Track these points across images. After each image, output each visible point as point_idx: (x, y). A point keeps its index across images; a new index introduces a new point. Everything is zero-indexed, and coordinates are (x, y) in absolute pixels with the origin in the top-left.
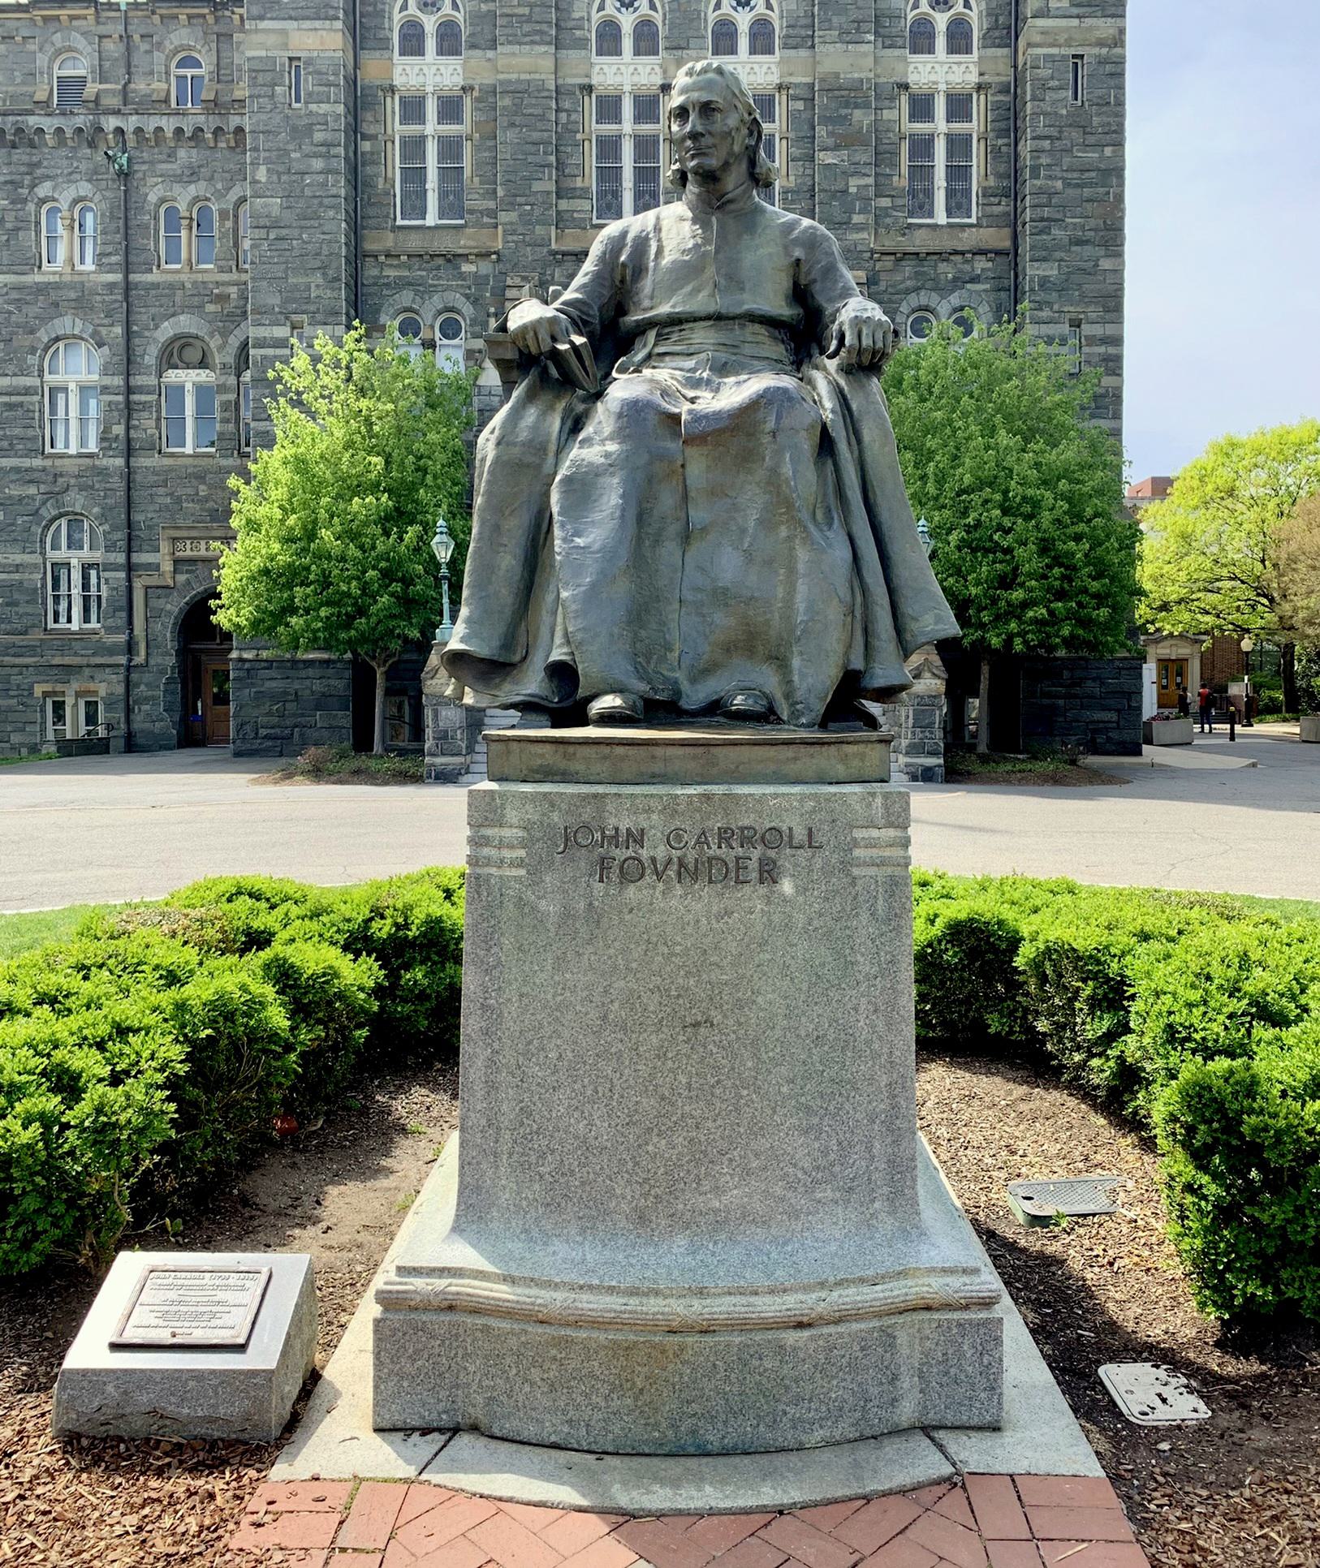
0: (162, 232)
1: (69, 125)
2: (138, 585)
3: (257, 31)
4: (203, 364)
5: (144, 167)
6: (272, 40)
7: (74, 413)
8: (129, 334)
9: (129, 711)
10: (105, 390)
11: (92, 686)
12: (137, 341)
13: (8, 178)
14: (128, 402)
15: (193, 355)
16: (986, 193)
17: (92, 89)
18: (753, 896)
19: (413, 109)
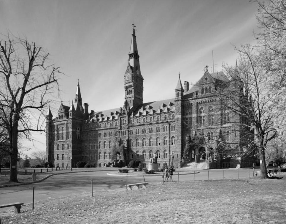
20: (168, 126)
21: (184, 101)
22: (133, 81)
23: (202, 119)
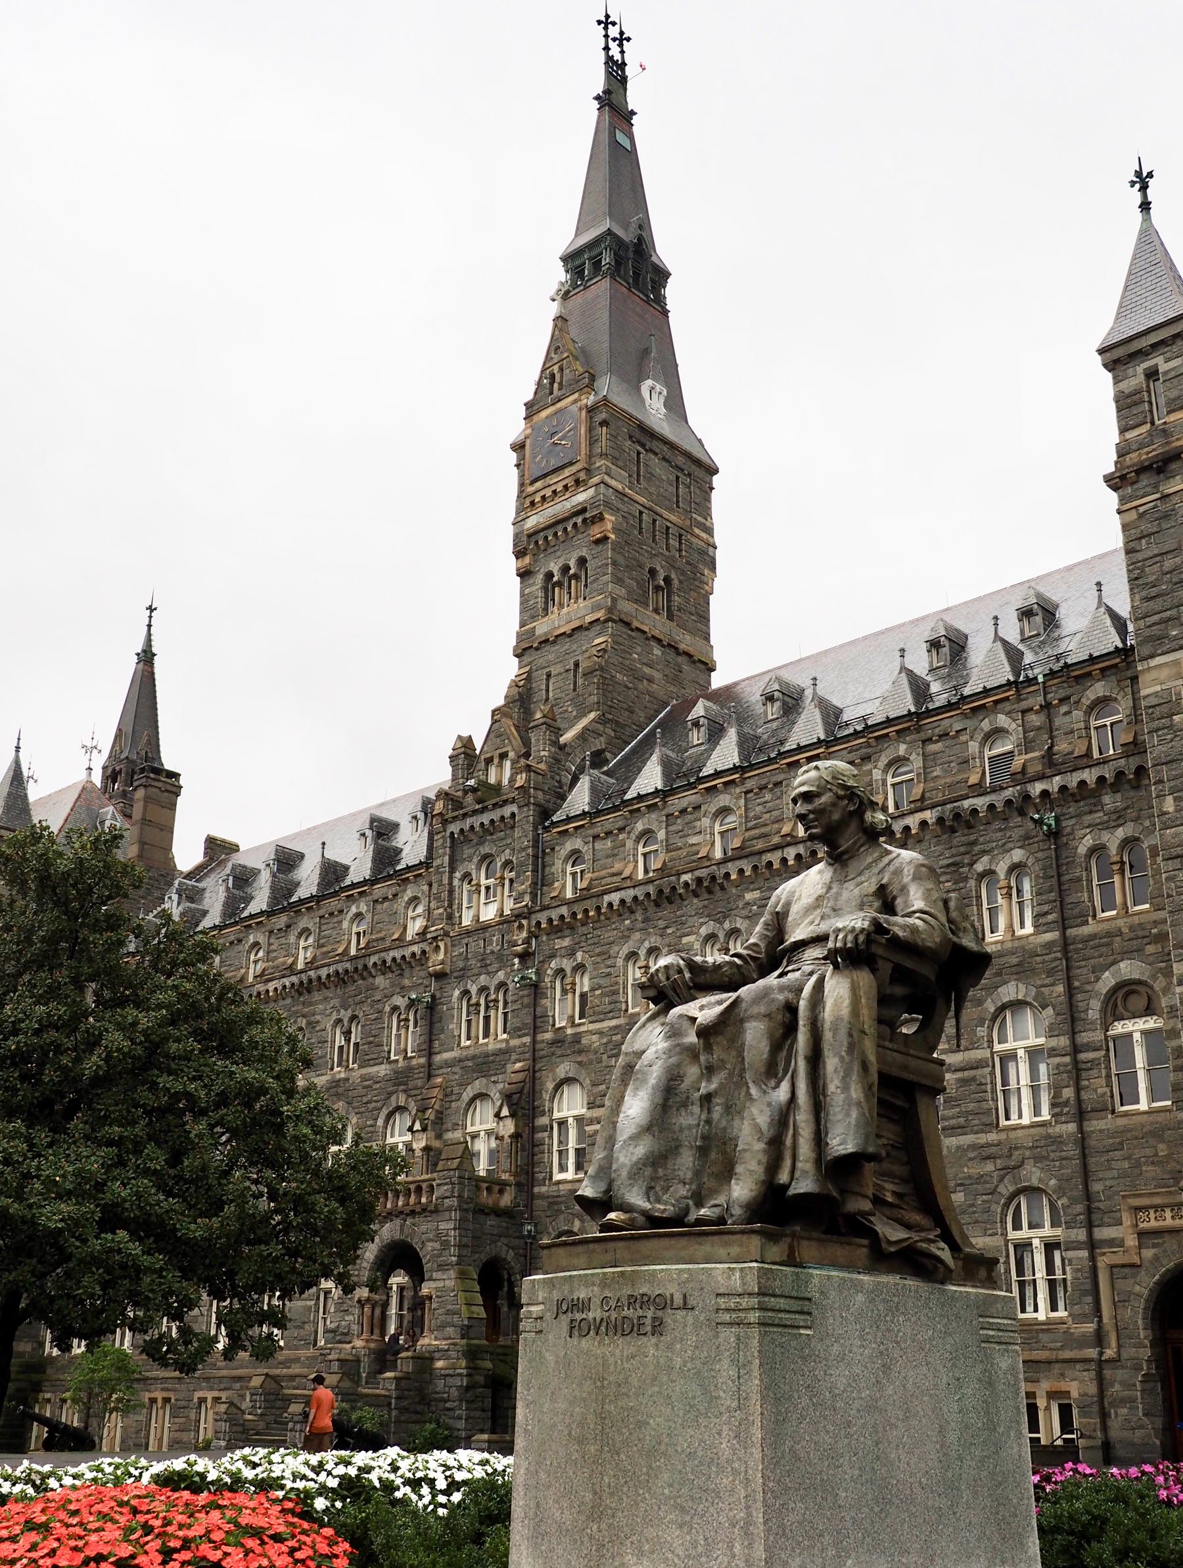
0: (1095, 882)
1: (998, 799)
2: (1103, 1262)
3: (1149, 669)
4: (1149, 1010)
5: (1073, 821)
6: (1164, 673)
7: (1025, 1079)
8: (1070, 991)
9: (1104, 1416)
10: (1053, 1052)
11: (1063, 1386)
12: (1079, 997)
13: (951, 861)
14: (1076, 1062)
15: (1139, 1002)
17: (1018, 762)
18: (649, 1344)
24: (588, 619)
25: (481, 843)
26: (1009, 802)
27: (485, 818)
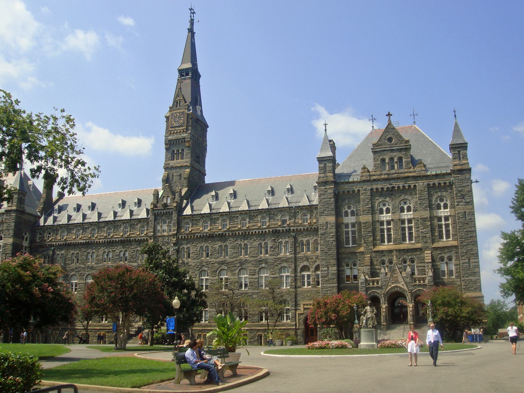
4: (309, 270)
6: (323, 219)
16: (452, 235)
19: (347, 226)
20: (291, 240)
21: (339, 183)
22: (190, 128)
23: (385, 227)
24: (185, 164)
25: (162, 216)
26: (286, 230)
27: (165, 211)
